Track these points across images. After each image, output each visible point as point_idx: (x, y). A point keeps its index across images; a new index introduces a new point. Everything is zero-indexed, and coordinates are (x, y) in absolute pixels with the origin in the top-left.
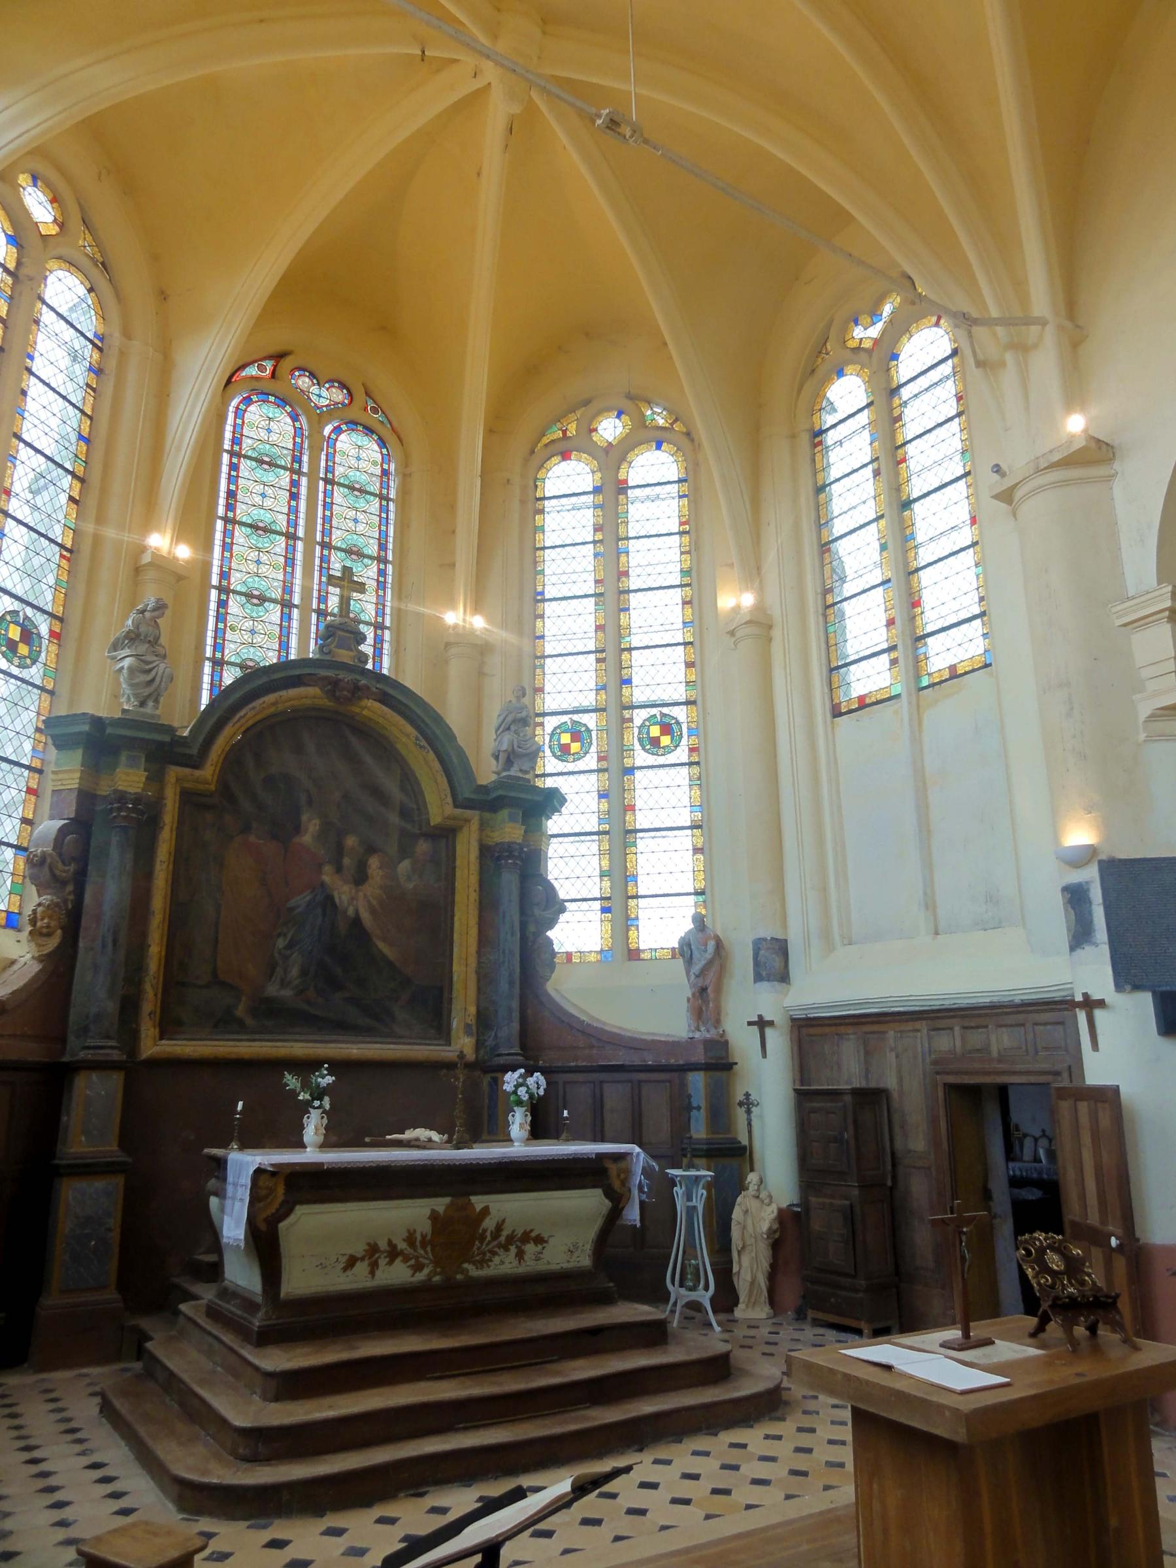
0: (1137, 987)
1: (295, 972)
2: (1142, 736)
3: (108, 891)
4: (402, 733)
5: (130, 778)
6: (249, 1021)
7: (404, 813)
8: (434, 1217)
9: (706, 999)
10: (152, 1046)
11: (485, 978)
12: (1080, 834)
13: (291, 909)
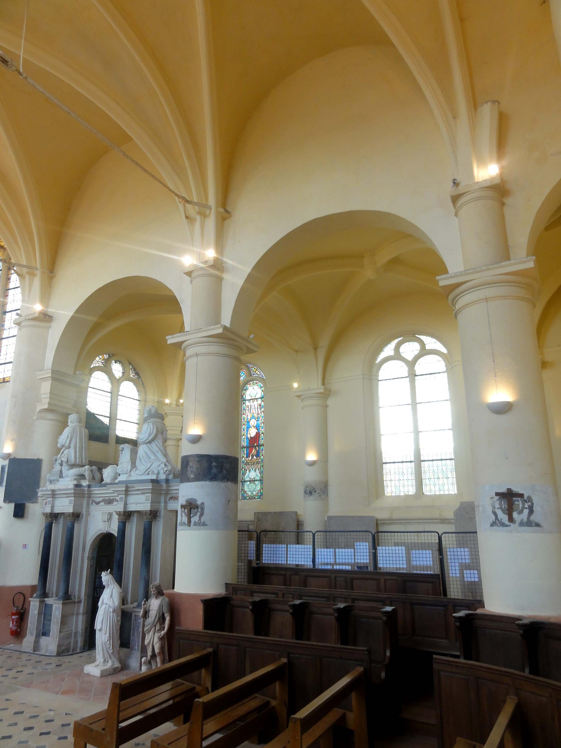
0: (10, 502)
2: (35, 418)
12: (8, 448)
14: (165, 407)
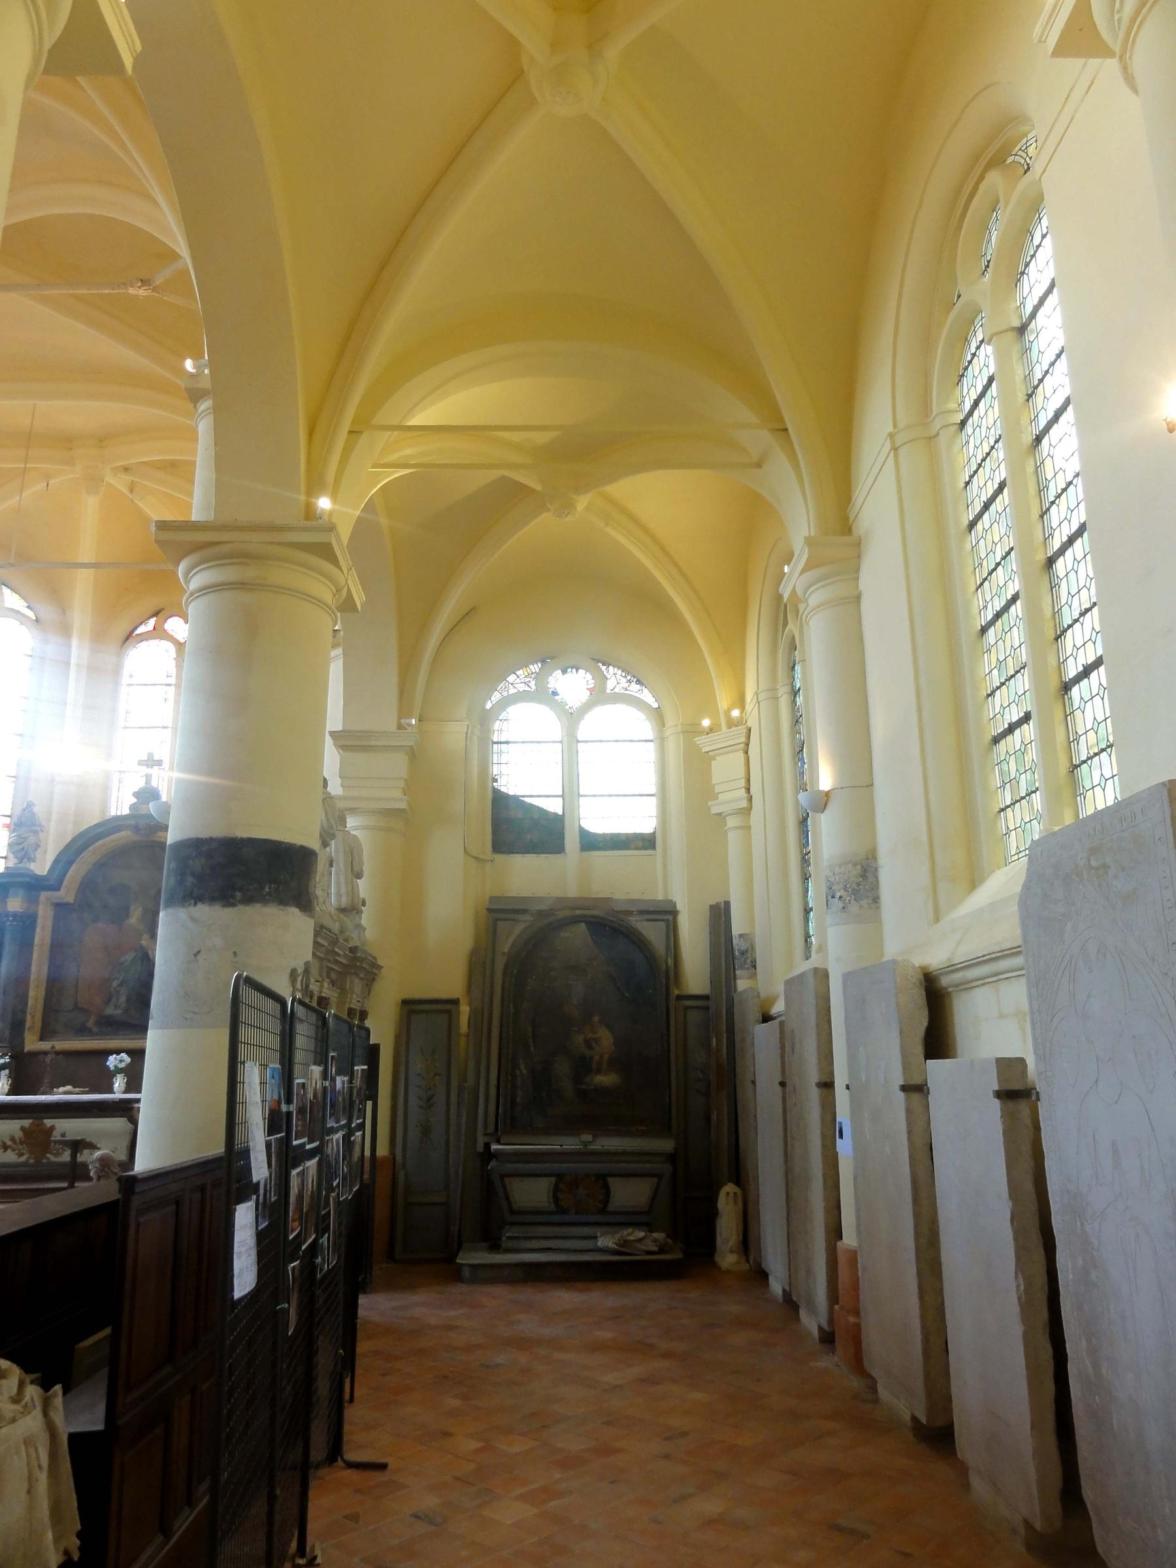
1: (123, 999)
6: (95, 1030)
8: (23, 1129)
10: (32, 1043)
13: (122, 963)
14: (700, 740)
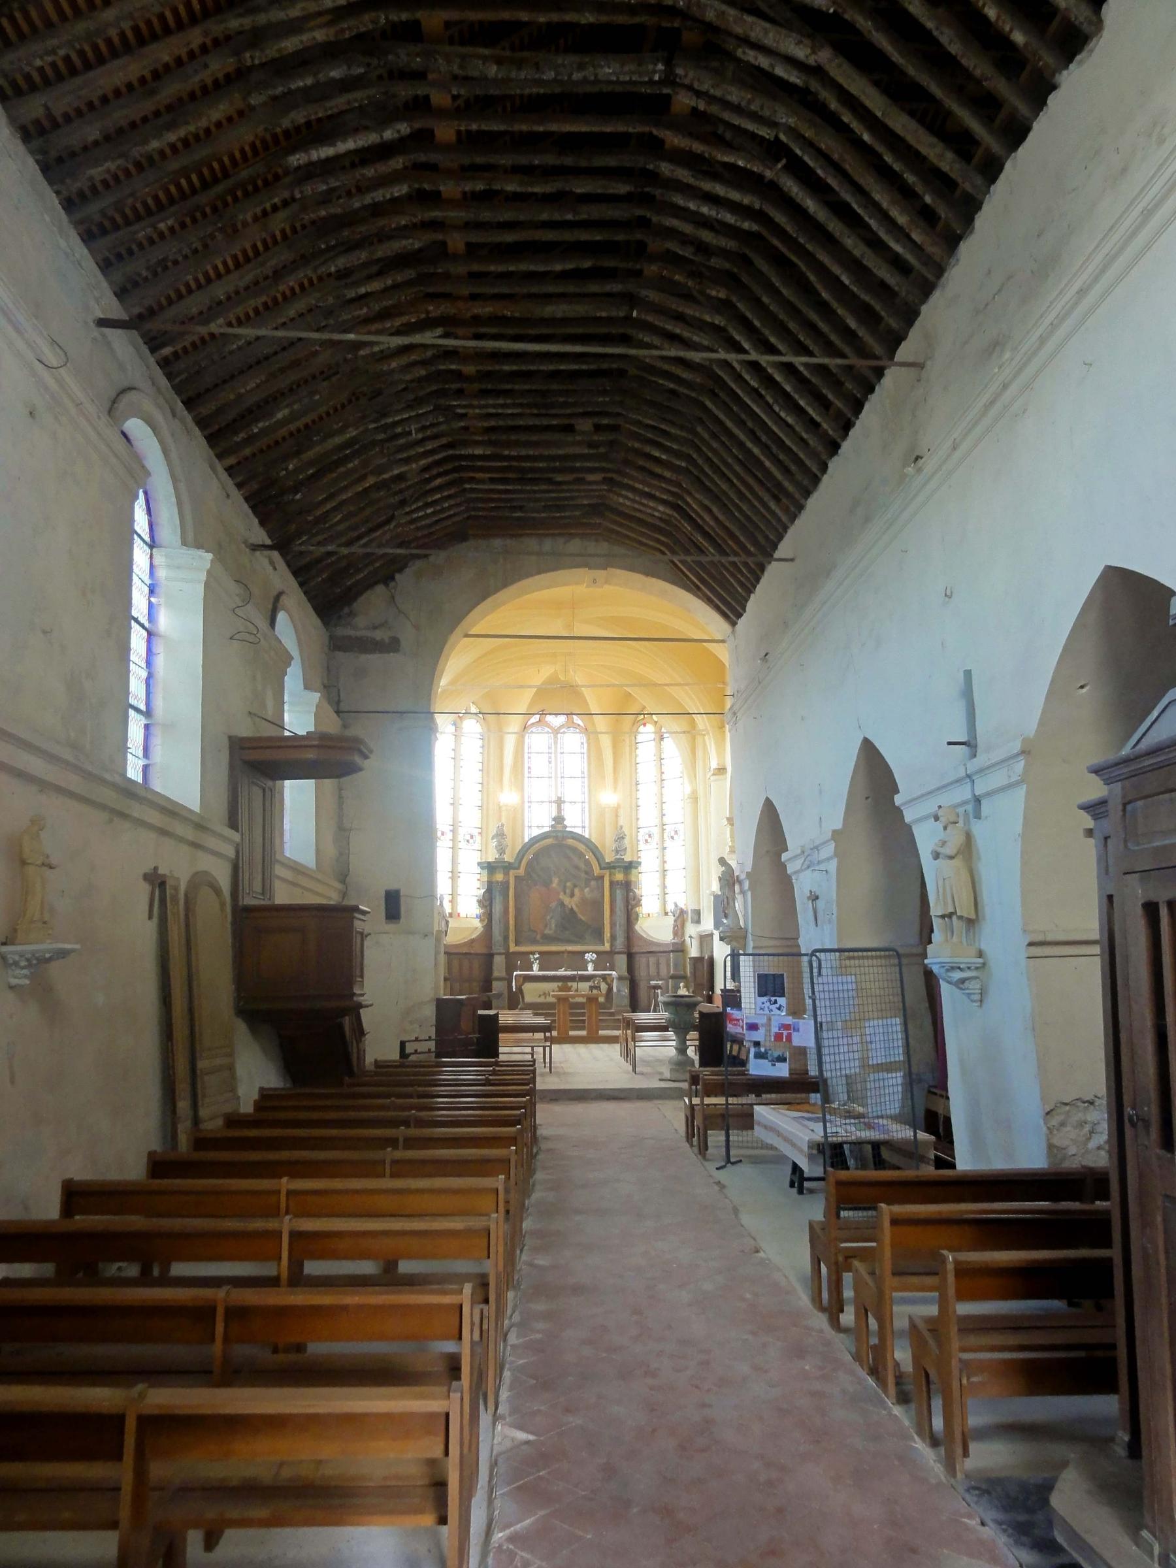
3: (497, 908)
4: (582, 847)
5: (499, 877)
7: (586, 873)
9: (679, 929)
10: (513, 948)
11: (613, 925)
